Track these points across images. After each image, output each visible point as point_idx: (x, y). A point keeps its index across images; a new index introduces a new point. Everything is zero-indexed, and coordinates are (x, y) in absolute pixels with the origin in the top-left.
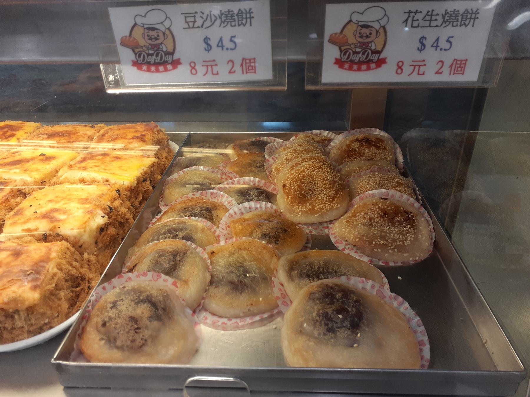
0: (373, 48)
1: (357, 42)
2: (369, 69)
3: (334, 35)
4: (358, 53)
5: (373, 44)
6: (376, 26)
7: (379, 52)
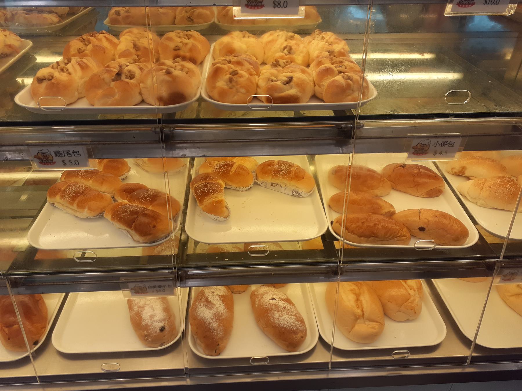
7: (53, 160)
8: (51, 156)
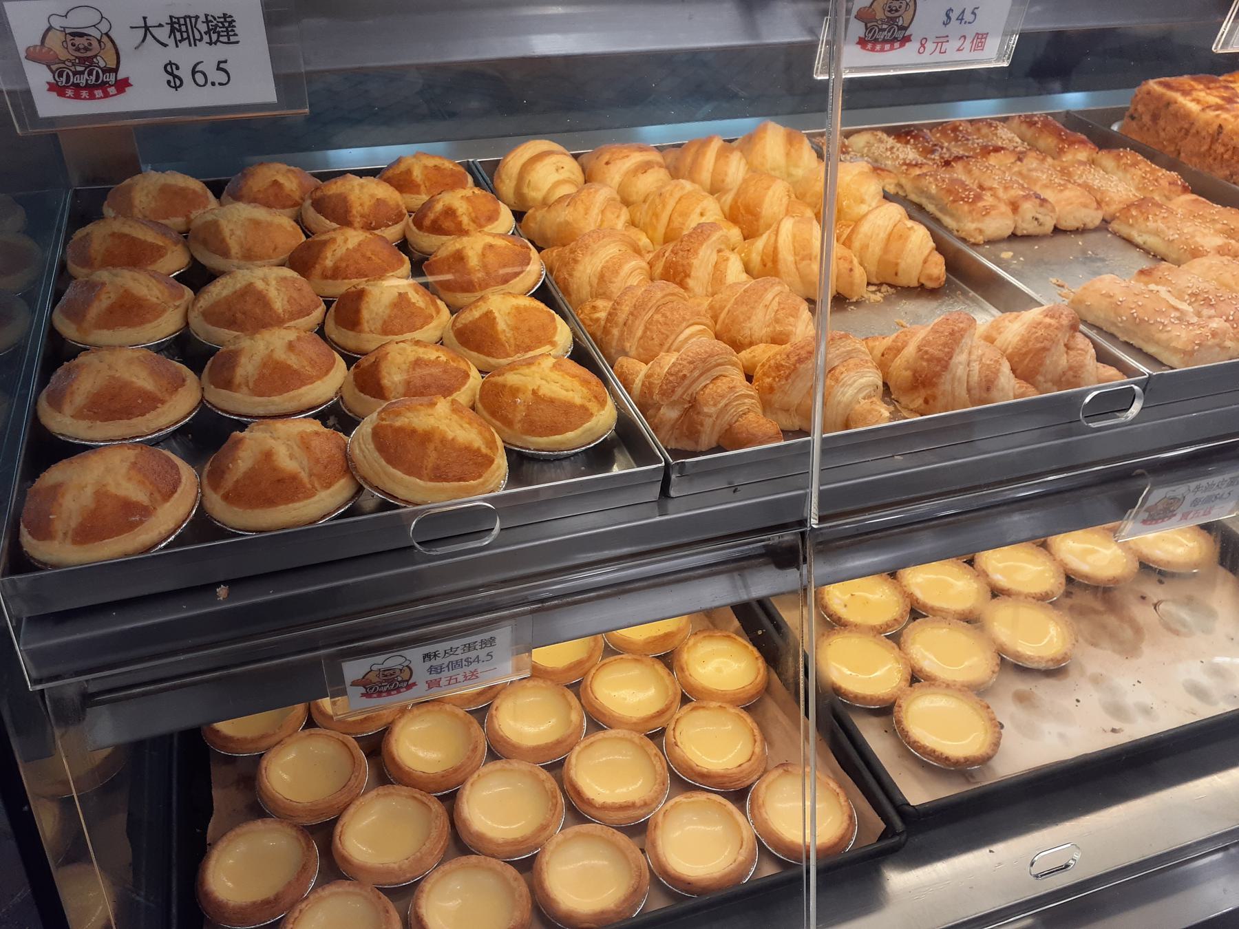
0: (102, 64)
1: (74, 58)
2: (106, 95)
3: (32, 49)
4: (82, 73)
5: (98, 58)
6: (92, 32)
7: (116, 70)
8: (109, 44)
